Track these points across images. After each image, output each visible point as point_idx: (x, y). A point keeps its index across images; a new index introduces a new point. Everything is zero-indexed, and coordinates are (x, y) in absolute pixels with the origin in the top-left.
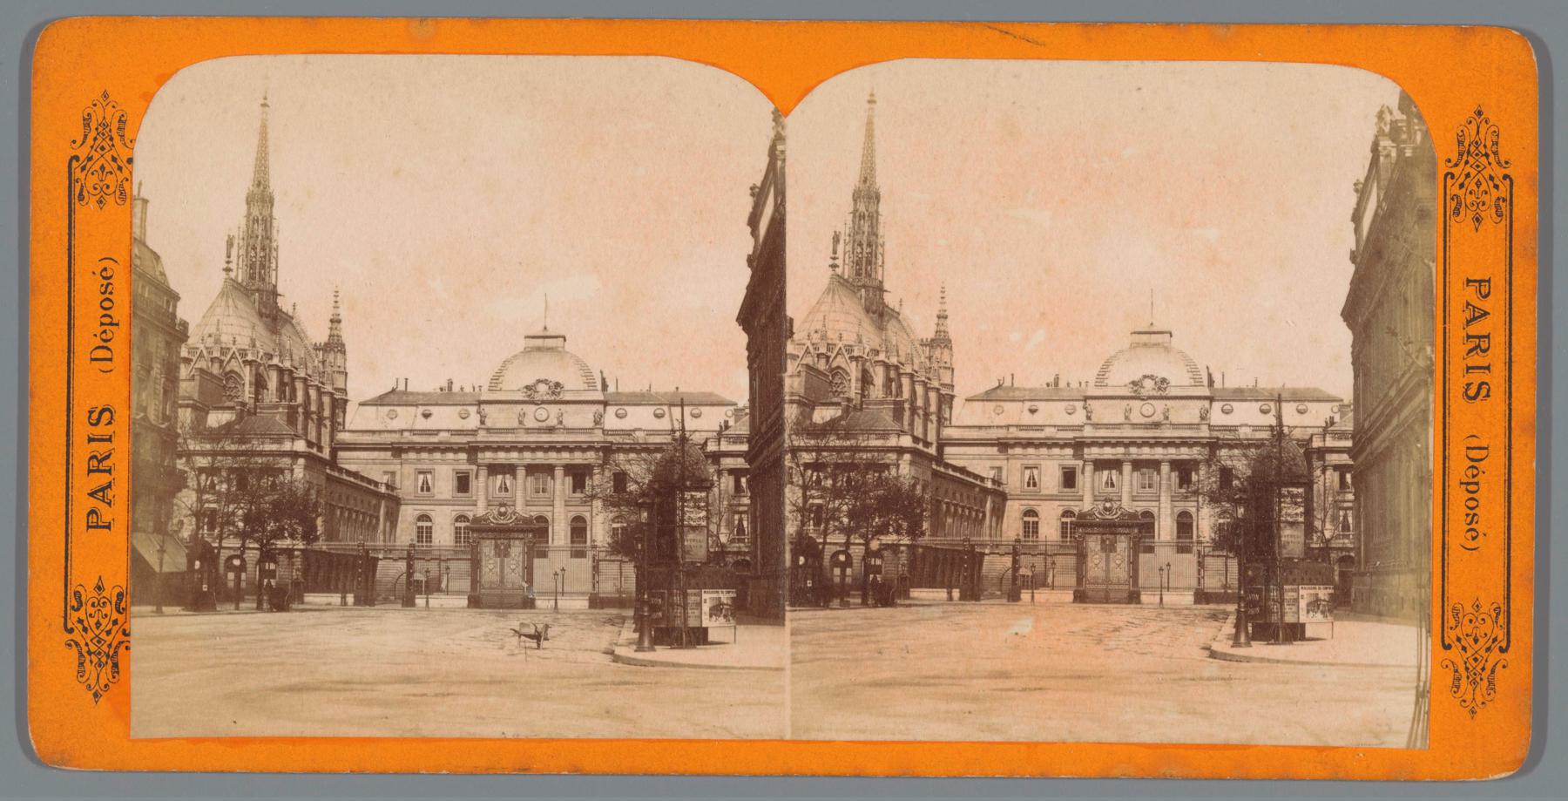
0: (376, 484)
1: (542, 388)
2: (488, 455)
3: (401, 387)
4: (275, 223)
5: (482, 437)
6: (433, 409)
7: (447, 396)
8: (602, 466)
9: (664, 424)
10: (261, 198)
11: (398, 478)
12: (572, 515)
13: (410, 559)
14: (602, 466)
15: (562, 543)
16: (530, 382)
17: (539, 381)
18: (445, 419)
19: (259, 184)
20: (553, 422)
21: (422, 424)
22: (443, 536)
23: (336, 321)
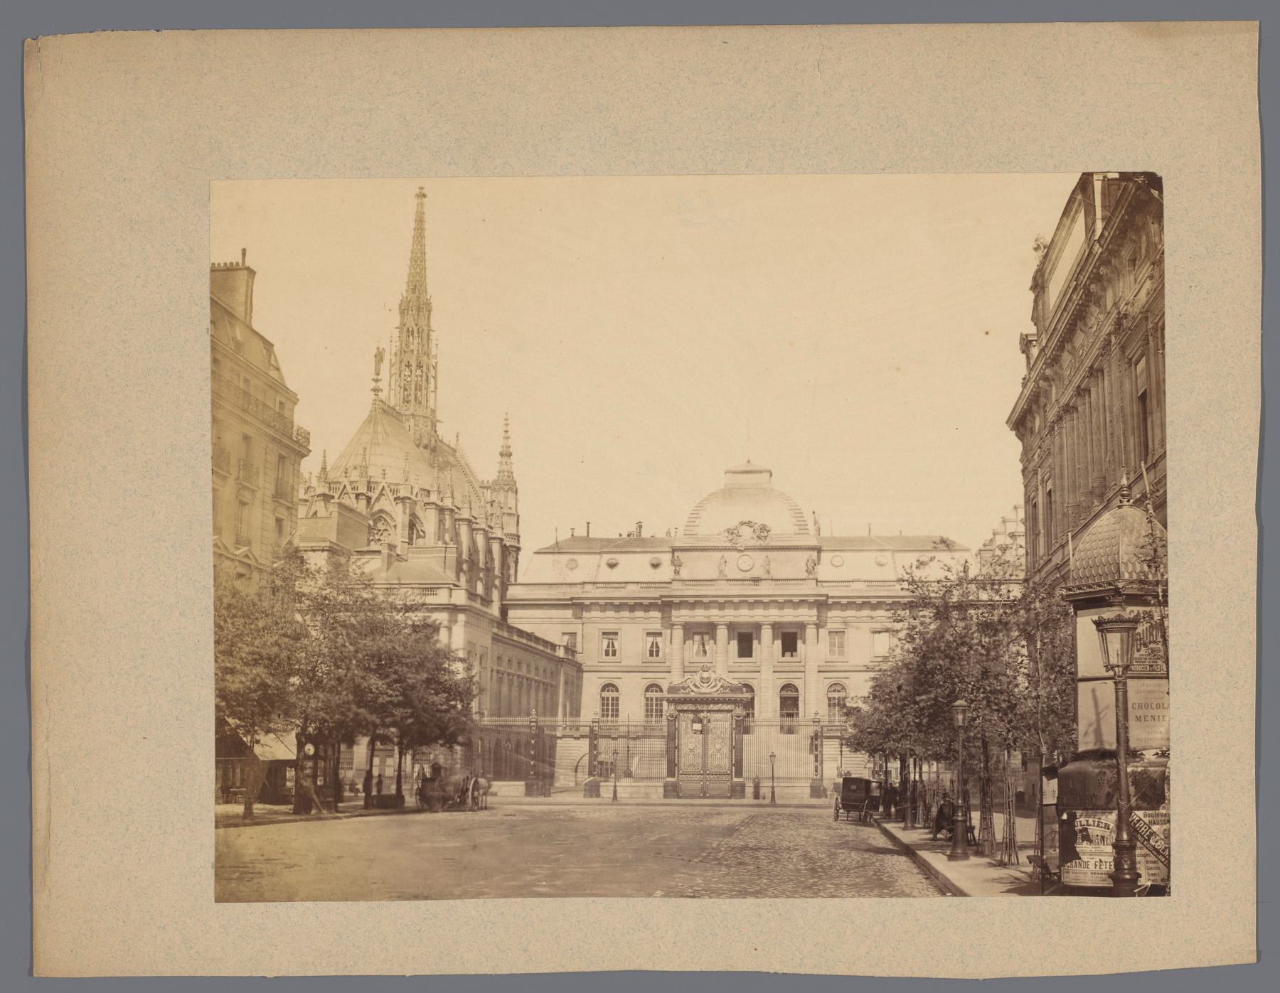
0: (553, 646)
1: (746, 532)
2: (684, 612)
3: (581, 532)
4: (433, 336)
5: (678, 590)
6: (619, 557)
7: (634, 542)
8: (818, 626)
9: (889, 574)
10: (416, 308)
11: (579, 638)
12: (781, 683)
13: (593, 736)
14: (818, 626)
15: (770, 715)
16: (733, 523)
17: (742, 523)
18: (634, 569)
19: (414, 290)
20: (758, 572)
21: (607, 575)
22: (632, 709)
23: (506, 454)
